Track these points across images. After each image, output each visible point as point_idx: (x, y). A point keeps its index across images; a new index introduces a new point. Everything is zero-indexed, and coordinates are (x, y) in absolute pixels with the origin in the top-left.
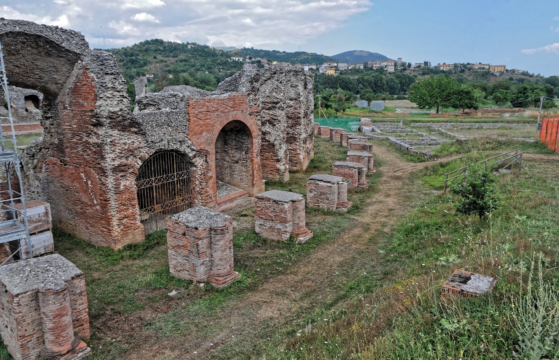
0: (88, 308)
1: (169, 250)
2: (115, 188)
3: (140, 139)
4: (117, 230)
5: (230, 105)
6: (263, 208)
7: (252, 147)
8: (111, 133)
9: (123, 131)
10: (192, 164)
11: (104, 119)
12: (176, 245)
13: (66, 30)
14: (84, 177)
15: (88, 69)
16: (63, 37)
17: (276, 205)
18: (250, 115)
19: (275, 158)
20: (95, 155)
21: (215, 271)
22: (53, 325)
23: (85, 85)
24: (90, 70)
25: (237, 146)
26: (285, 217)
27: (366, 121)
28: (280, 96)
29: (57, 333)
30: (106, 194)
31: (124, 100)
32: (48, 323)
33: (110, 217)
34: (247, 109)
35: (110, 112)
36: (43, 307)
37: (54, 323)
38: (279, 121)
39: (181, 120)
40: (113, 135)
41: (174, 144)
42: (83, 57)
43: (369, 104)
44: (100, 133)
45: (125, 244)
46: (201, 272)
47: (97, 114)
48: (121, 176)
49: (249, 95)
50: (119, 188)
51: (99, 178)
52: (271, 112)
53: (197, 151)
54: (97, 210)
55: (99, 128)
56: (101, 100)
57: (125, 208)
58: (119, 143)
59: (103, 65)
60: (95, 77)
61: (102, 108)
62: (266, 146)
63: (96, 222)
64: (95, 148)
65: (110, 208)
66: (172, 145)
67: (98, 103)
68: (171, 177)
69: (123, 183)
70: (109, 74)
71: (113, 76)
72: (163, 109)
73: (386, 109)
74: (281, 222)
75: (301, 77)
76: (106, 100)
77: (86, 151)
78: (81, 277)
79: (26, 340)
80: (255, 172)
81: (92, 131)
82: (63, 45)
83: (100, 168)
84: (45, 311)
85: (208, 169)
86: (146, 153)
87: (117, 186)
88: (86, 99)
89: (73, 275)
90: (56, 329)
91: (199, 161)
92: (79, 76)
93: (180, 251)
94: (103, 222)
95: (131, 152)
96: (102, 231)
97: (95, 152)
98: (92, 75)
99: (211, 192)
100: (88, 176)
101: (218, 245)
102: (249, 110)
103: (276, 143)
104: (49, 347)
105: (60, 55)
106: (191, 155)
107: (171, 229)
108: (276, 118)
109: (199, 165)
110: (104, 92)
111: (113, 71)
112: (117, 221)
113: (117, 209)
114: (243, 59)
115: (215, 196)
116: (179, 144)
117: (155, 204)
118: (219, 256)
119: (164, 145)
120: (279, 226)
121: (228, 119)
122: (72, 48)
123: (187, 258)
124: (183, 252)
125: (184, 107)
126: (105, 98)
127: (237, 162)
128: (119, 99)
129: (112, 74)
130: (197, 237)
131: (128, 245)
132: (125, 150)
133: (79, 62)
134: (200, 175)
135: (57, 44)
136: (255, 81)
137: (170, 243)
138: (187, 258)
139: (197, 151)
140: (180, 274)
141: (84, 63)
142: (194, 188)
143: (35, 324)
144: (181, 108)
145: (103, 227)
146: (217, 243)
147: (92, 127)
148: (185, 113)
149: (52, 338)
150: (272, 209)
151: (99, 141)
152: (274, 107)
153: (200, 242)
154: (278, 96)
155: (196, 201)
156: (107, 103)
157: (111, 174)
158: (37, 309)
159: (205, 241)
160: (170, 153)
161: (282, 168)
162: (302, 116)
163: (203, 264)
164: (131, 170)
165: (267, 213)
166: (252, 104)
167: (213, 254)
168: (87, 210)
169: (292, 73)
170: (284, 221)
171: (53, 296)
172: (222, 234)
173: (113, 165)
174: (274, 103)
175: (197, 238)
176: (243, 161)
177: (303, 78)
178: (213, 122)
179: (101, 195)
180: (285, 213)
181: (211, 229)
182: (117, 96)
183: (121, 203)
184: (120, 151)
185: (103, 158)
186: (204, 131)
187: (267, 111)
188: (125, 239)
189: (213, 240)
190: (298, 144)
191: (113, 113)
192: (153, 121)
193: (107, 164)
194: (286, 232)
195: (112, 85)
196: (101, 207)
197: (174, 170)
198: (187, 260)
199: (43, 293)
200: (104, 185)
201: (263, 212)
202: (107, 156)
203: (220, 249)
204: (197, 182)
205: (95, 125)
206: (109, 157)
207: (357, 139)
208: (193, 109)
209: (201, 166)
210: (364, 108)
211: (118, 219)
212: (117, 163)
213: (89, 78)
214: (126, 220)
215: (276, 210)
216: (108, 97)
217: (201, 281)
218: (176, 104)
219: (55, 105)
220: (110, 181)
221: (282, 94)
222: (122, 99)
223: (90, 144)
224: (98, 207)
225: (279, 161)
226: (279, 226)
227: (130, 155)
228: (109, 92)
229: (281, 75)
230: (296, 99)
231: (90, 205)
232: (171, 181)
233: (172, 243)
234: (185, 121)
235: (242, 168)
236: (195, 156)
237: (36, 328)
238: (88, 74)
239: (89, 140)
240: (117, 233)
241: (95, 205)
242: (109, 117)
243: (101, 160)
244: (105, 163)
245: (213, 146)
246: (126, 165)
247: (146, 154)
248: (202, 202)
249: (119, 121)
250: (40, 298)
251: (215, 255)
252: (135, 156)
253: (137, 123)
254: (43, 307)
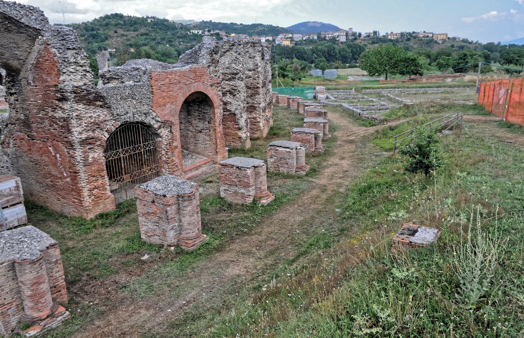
0: (64, 275)
1: (139, 217)
2: (84, 160)
3: (105, 113)
4: (88, 201)
5: (192, 77)
6: (227, 174)
7: (215, 117)
8: (77, 108)
9: (89, 105)
10: (158, 135)
11: (69, 94)
12: (146, 212)
13: (25, 6)
14: (52, 151)
15: (50, 44)
16: (22, 13)
17: (238, 171)
18: (211, 86)
19: (237, 126)
20: (62, 129)
21: (184, 235)
22: (31, 292)
23: (47, 60)
24: (52, 45)
25: (200, 116)
26: (248, 181)
27: (321, 89)
28: (239, 67)
29: (36, 300)
30: (75, 167)
31: (88, 74)
32: (26, 291)
33: (81, 189)
34: (208, 80)
35: (74, 86)
36: (20, 276)
37: (32, 290)
38: (239, 91)
39: (145, 92)
40: (79, 109)
41: (139, 116)
42: (43, 32)
43: (323, 73)
44: (66, 108)
45: (97, 213)
46: (171, 236)
47: (61, 89)
48: (89, 149)
49: (209, 66)
50: (87, 160)
51: (67, 152)
52: (231, 83)
53: (162, 123)
54: (67, 182)
55: (64, 102)
56: (65, 75)
57: (94, 179)
58: (84, 117)
59: (64, 40)
60: (57, 53)
61: (66, 83)
62: (228, 115)
63: (67, 194)
64: (62, 122)
65: (80, 180)
66: (138, 117)
67: (62, 78)
68: (138, 148)
69: (91, 155)
70: (70, 49)
71: (75, 51)
72: (127, 83)
73: (339, 77)
74: (245, 187)
75: (258, 48)
76: (70, 75)
77: (52, 125)
78: (55, 246)
79: (5, 308)
80: (218, 140)
81: (57, 106)
82: (23, 20)
83: (67, 142)
84: (22, 280)
85: (173, 139)
86: (112, 126)
87: (86, 159)
88: (49, 74)
89: (48, 245)
90: (35, 296)
91: (164, 132)
92: (40, 52)
93: (149, 218)
94: (74, 193)
95: (97, 125)
96: (74, 202)
97: (62, 126)
98: (54, 50)
99: (177, 161)
100: (56, 150)
101: (186, 210)
102: (210, 82)
103: (237, 112)
104: (28, 313)
105: (20, 31)
106: (156, 126)
107: (141, 198)
108: (236, 88)
109: (164, 136)
110: (67, 67)
111: (74, 46)
112: (88, 192)
113: (87, 181)
114: (202, 32)
115: (182, 165)
116: (144, 116)
117: (124, 174)
118: (187, 221)
119: (129, 118)
120: (242, 191)
121: (190, 90)
122: (32, 23)
123: (157, 224)
124: (153, 218)
125: (146, 80)
126: (68, 73)
127: (201, 132)
128: (83, 74)
129: (74, 49)
130: (166, 204)
131: (100, 214)
132: (91, 123)
133: (40, 37)
134: (166, 145)
135: (15, 20)
136: (215, 54)
137: (140, 210)
138: (157, 224)
139: (162, 123)
140: (151, 239)
141: (44, 38)
142: (160, 158)
143: (13, 293)
144: (144, 81)
145: (74, 198)
146: (185, 209)
147: (57, 102)
148: (148, 86)
149: (31, 305)
150: (235, 175)
151: (65, 116)
152: (234, 78)
153: (168, 209)
154: (236, 67)
155: (163, 170)
156: (70, 78)
158: (15, 278)
159: (174, 207)
160: (135, 125)
161: (244, 136)
162: (260, 86)
163: (172, 229)
164: (98, 143)
165: (231, 178)
166: (212, 75)
167: (182, 219)
168: (58, 182)
169: (250, 45)
170: (247, 186)
171: (29, 266)
172: (189, 200)
173: (80, 138)
174: (233, 74)
175: (166, 205)
176: (207, 131)
177: (260, 49)
178: (176, 93)
179: (70, 168)
180: (248, 177)
181: (178, 196)
182: (80, 71)
183: (91, 175)
184: (86, 125)
185: (69, 131)
186: (168, 102)
187: (227, 82)
188: (96, 208)
189: (181, 206)
190: (258, 112)
191: (77, 87)
192: (117, 94)
193: (74, 138)
194: (249, 196)
195: (74, 60)
196: (72, 179)
197: (140, 141)
198: (157, 226)
199: (19, 263)
200: (73, 157)
201: (227, 178)
202: (73, 130)
203: (188, 215)
204: (163, 152)
205: (60, 100)
206: (76, 130)
207: (313, 107)
208: (156, 82)
209: (166, 137)
210: (318, 77)
211: (89, 190)
212: (84, 136)
213: (50, 53)
214: (96, 190)
215: (239, 176)
216: (71, 72)
217: (172, 245)
218: (139, 77)
219: (18, 81)
220: (79, 154)
222: (85, 73)
223: (57, 119)
224: (68, 179)
225: (240, 130)
226: (242, 191)
227: (97, 128)
228: (72, 67)
229: (240, 47)
230: (254, 70)
231: (60, 178)
232: (137, 152)
233: (142, 211)
234: (148, 93)
235: (205, 137)
236: (160, 127)
237: (15, 297)
238: (50, 49)
239: (55, 115)
240: (88, 204)
241: (66, 178)
242: (73, 92)
243: (68, 134)
244: (72, 137)
245: (177, 117)
246: (93, 138)
247: (113, 127)
248: (169, 171)
249: (83, 95)
250: (17, 268)
251: (183, 219)
252: (101, 129)
253: (102, 97)
254: (20, 276)
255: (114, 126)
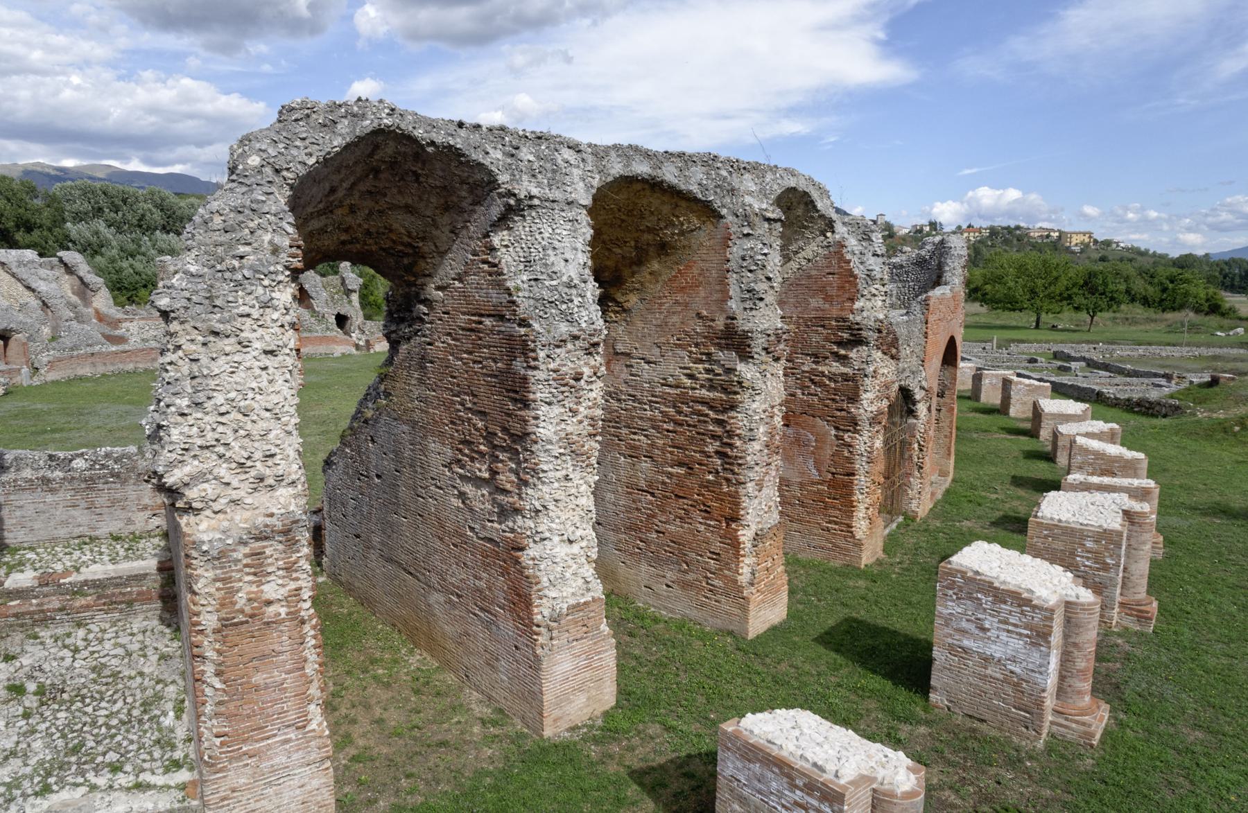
33: (855, 504)
56: (862, 299)
61: (865, 314)
67: (858, 305)
70: (878, 255)
106: (918, 397)
126: (869, 297)
141: (837, 236)
142: (911, 457)
145: (830, 522)
157: (867, 427)
173: (872, 412)
193: (862, 411)
200: (850, 446)
202: (864, 396)
239: (820, 369)
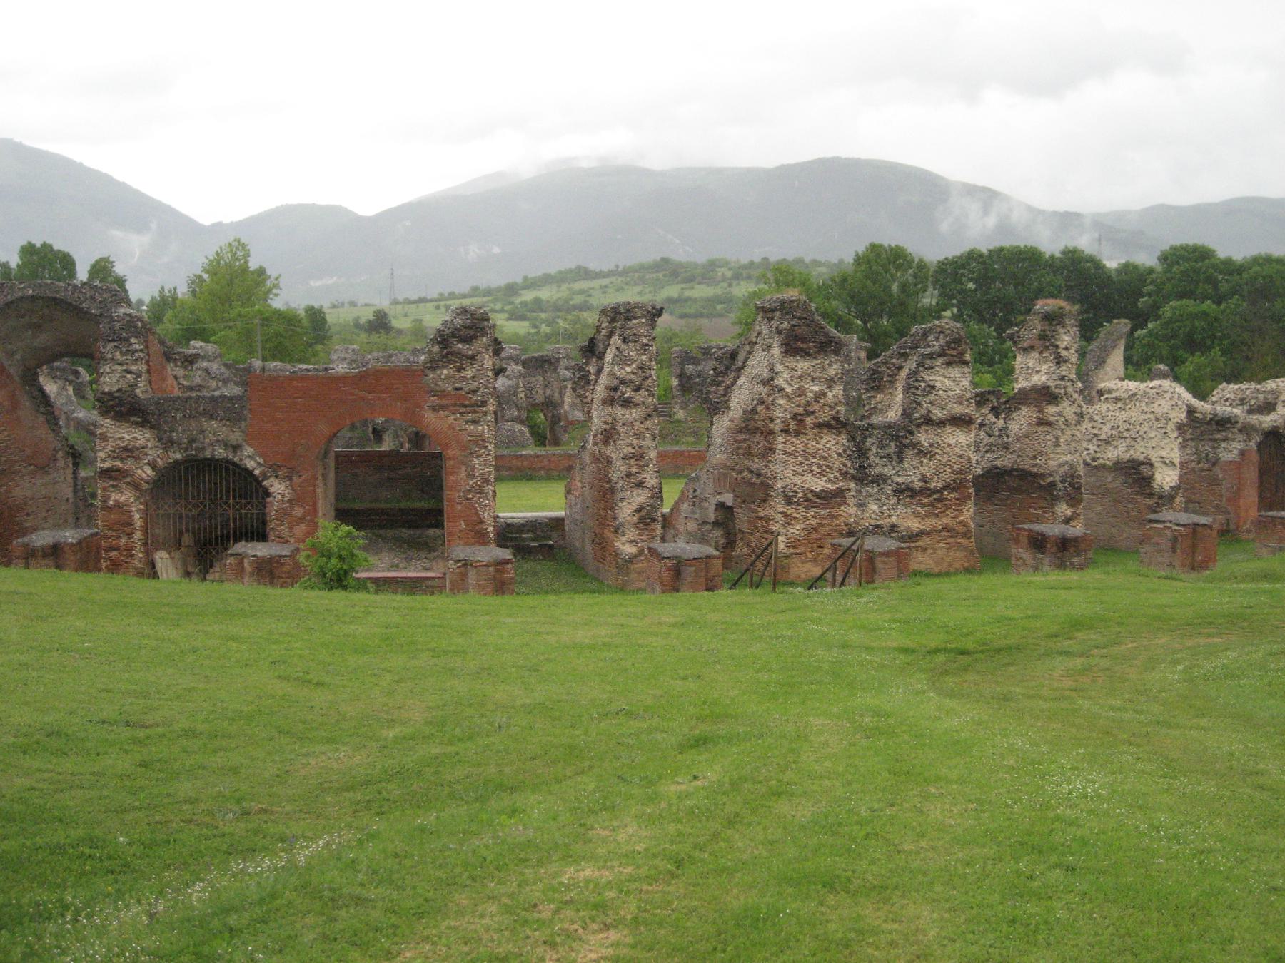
31: (129, 376)
95: (129, 452)
164: (128, 480)
197: (228, 492)
207: (1161, 526)
212: (106, 465)
221: (628, 369)
222: (124, 374)
227: (129, 456)
255: (162, 459)
